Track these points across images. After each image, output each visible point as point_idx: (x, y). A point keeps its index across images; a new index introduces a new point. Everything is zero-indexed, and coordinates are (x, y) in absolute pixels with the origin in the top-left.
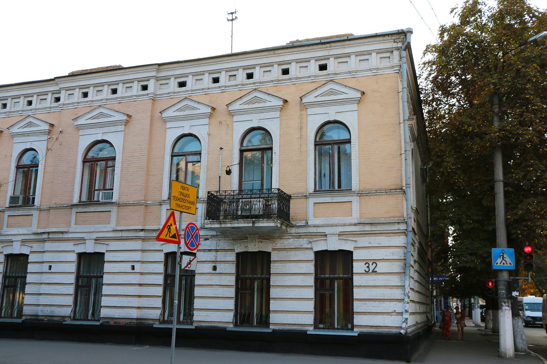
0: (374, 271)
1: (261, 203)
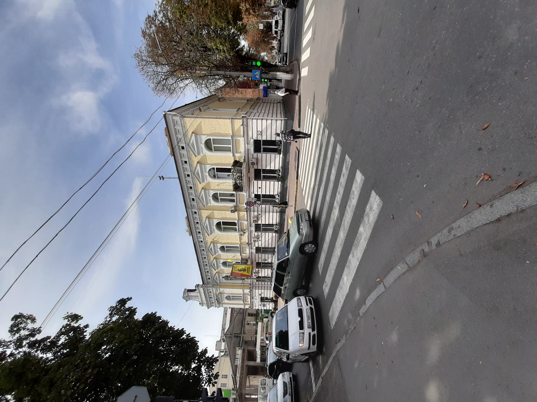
0: (261, 132)
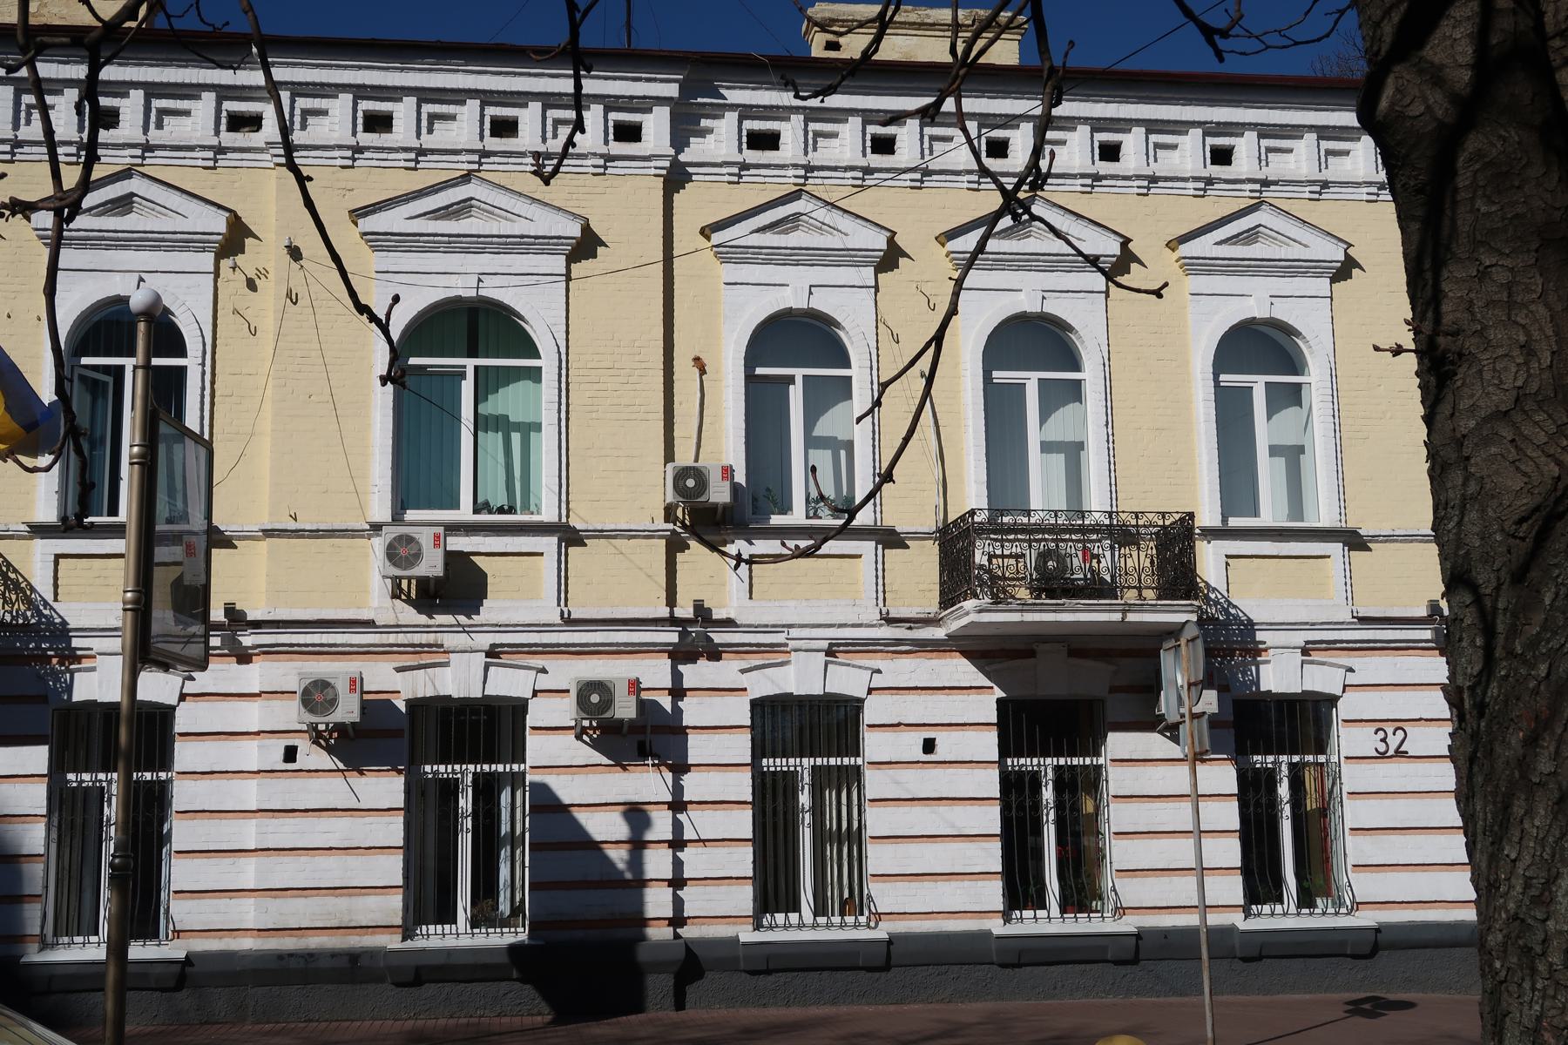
1: (1142, 555)
